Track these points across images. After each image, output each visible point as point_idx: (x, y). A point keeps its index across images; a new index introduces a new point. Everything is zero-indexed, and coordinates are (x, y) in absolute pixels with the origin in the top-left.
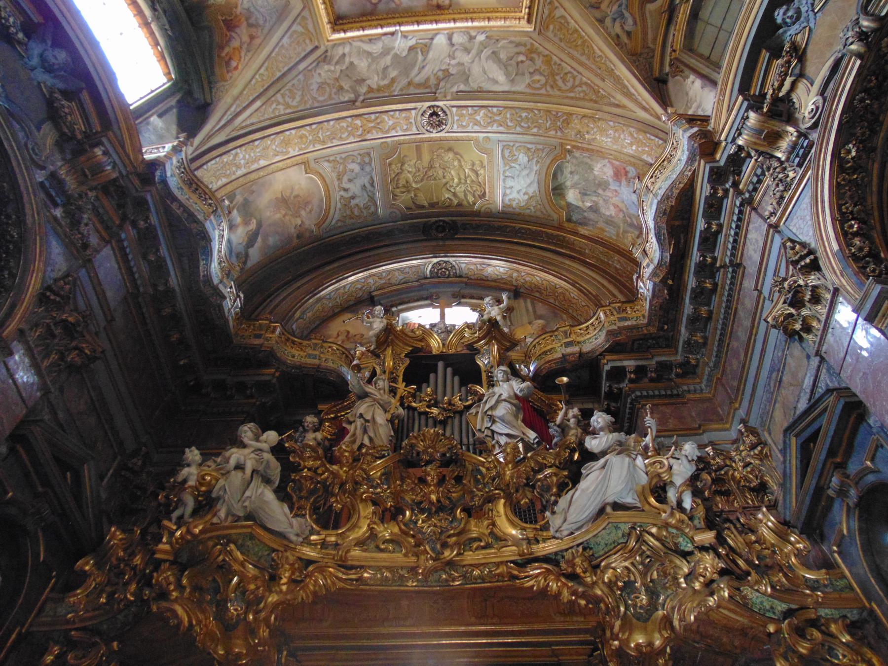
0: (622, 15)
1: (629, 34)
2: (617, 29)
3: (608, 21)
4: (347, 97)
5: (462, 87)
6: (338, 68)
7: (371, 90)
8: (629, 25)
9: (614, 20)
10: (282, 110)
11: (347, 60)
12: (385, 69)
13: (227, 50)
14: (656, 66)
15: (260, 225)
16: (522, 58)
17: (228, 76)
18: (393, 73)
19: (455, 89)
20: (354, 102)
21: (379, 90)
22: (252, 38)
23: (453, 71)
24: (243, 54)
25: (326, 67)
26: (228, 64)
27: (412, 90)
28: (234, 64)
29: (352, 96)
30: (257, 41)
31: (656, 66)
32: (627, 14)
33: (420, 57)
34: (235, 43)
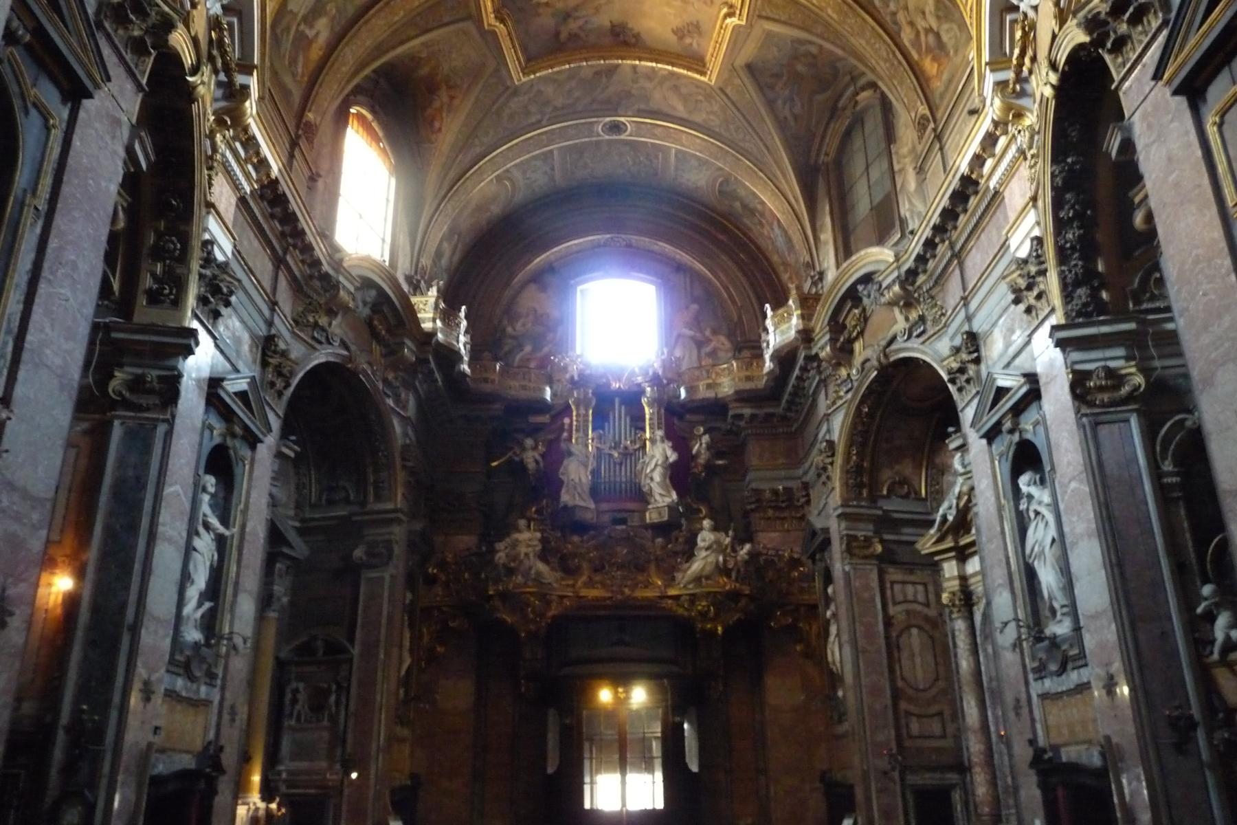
0: (792, 100)
1: (796, 118)
2: (787, 112)
3: (780, 102)
4: (533, 119)
5: (642, 106)
6: (526, 97)
7: (556, 109)
8: (798, 109)
9: (784, 103)
10: (478, 150)
11: (535, 88)
12: (570, 91)
13: (429, 111)
14: (813, 154)
15: (459, 235)
16: (700, 98)
17: (433, 137)
18: (577, 94)
19: (636, 107)
20: (539, 121)
21: (563, 108)
22: (452, 98)
23: (634, 91)
24: (444, 115)
25: (516, 99)
26: (431, 123)
27: (595, 106)
28: (437, 124)
29: (539, 117)
30: (456, 102)
31: (813, 154)
32: (796, 99)
33: (604, 80)
34: (437, 104)
